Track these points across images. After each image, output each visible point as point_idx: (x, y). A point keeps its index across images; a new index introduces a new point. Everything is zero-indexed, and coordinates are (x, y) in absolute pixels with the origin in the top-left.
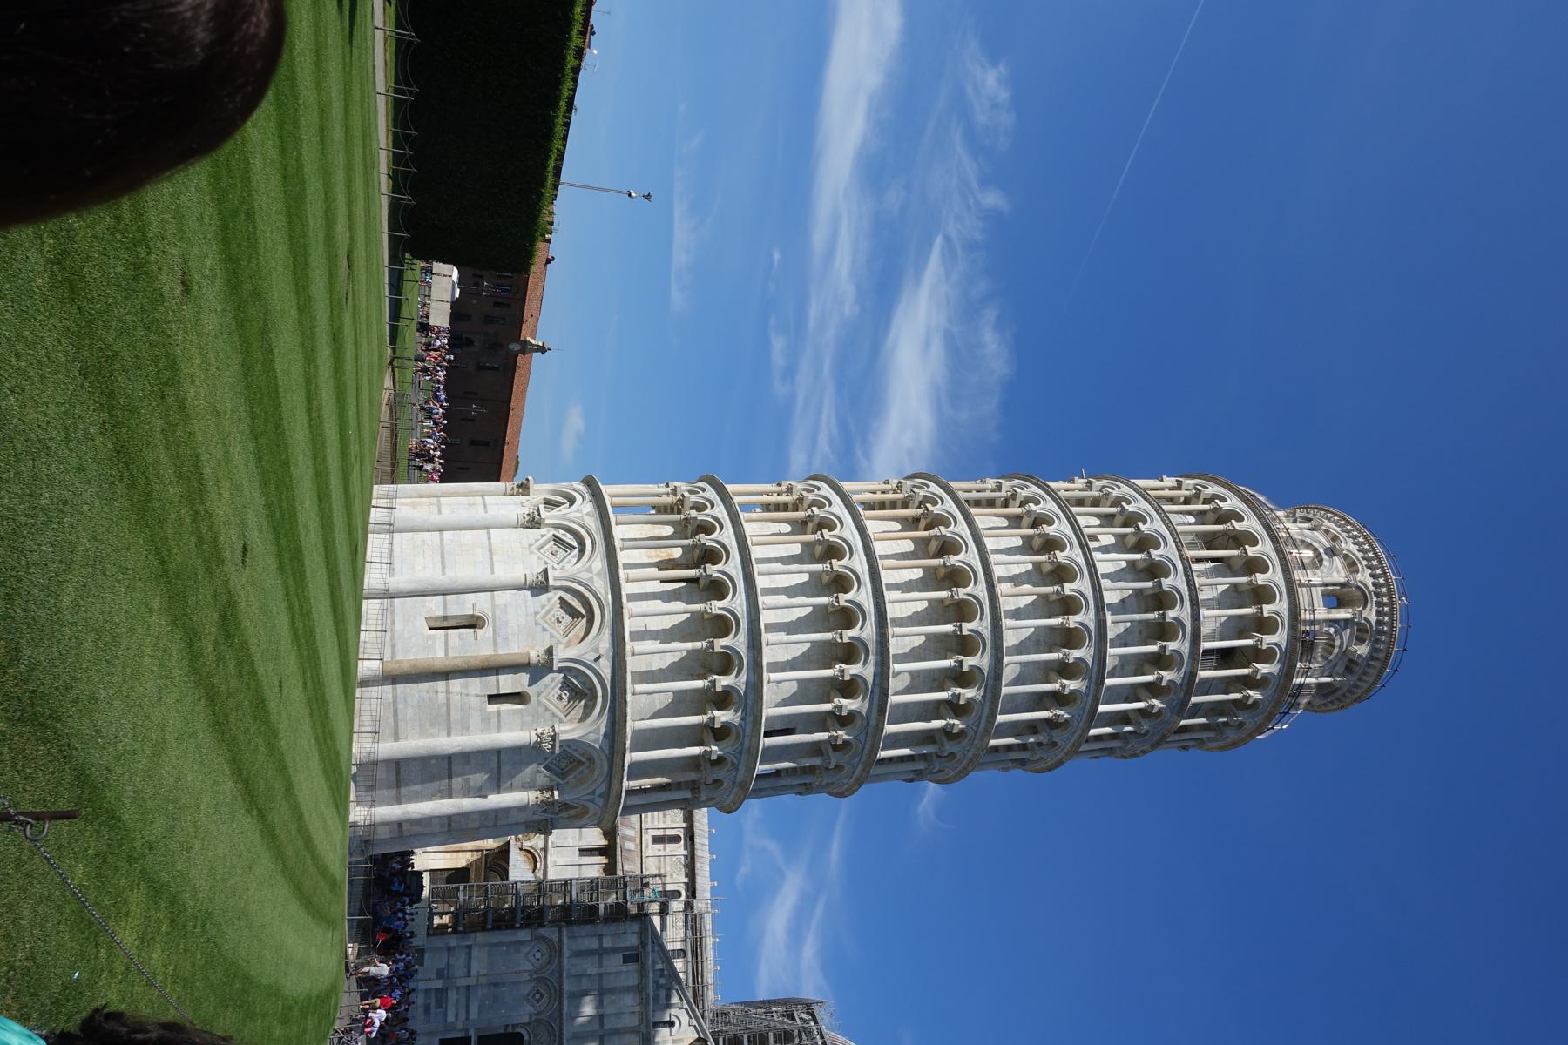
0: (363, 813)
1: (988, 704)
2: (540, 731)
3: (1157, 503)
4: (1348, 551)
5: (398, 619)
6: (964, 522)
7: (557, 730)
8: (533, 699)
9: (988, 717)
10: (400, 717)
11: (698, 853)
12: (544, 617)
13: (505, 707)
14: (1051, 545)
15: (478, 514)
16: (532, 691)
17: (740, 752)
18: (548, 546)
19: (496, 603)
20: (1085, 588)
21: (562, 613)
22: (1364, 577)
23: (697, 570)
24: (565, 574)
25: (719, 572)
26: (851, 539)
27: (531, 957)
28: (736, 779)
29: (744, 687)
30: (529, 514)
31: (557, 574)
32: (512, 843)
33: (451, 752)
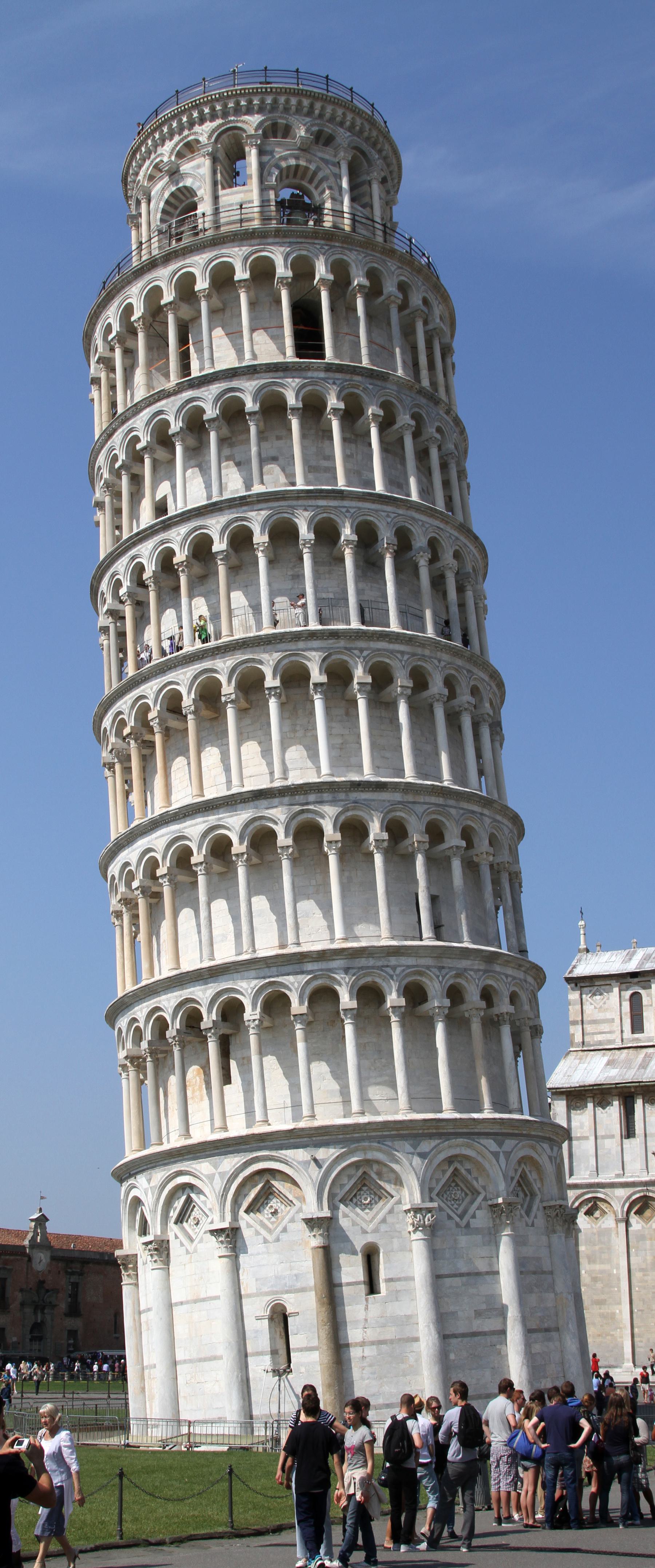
2: (411, 1228)
3: (117, 420)
4: (171, 153)
6: (143, 687)
7: (408, 1207)
8: (370, 1238)
9: (390, 642)
12: (270, 1231)
13: (383, 1273)
16: (359, 1242)
19: (255, 1291)
20: (218, 522)
23: (209, 1040)
24: (217, 1208)
28: (479, 970)
30: (152, 1255)
31: (216, 1216)
33: (437, 1336)
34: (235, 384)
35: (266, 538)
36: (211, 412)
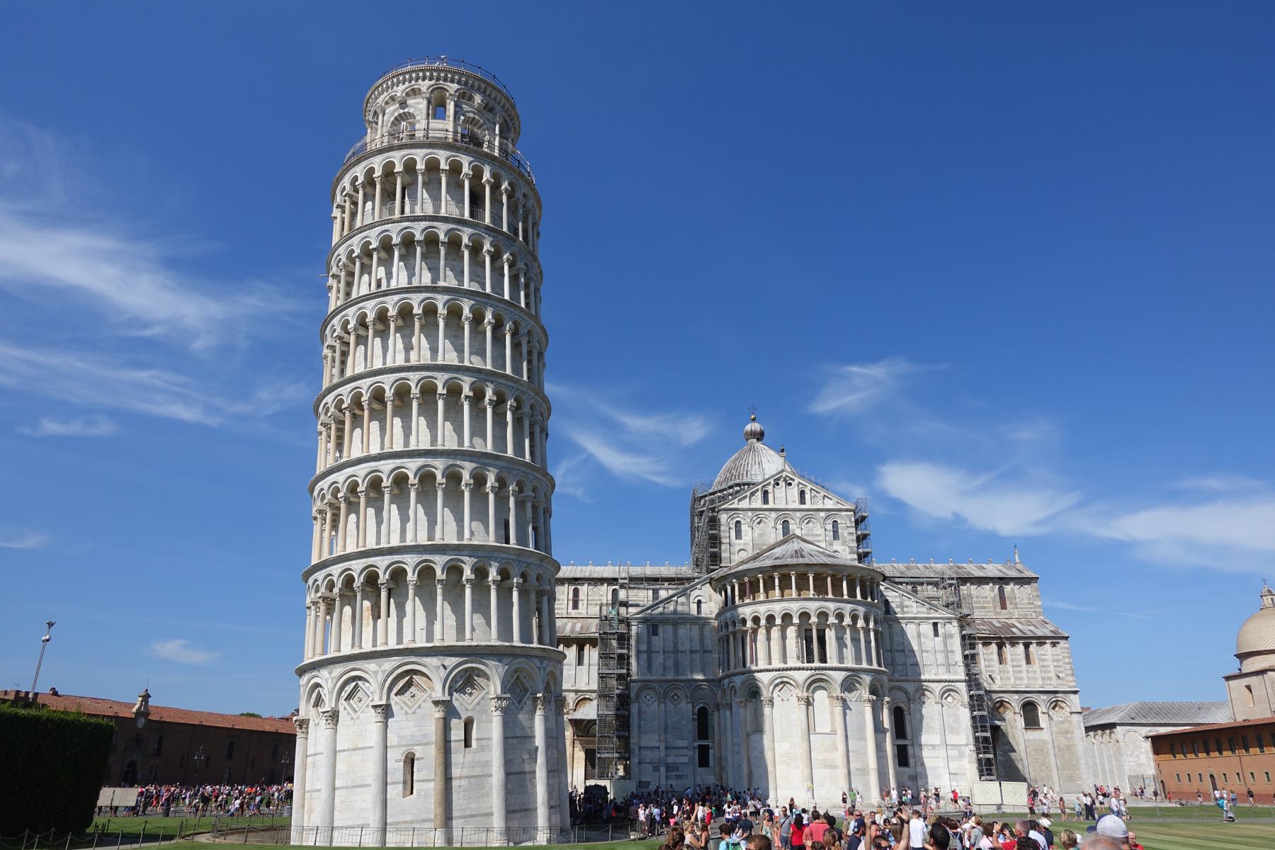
0: (542, 835)
1: (498, 380)
2: (493, 709)
3: (353, 232)
5: (402, 819)
6: (359, 382)
7: (493, 696)
8: (470, 714)
9: (507, 380)
10: (475, 813)
11: (587, 575)
12: (410, 707)
13: (474, 735)
14: (382, 316)
15: (323, 761)
16: (464, 715)
17: (519, 561)
18: (354, 706)
19: (396, 744)
20: (418, 298)
21: (408, 694)
22: (425, 85)
23: (382, 590)
24: (378, 692)
25: (385, 573)
26: (366, 470)
27: (651, 701)
29: (472, 559)
30: (327, 720)
31: (376, 697)
32: (570, 717)
34: (435, 224)
35: (445, 312)
36: (396, 240)
